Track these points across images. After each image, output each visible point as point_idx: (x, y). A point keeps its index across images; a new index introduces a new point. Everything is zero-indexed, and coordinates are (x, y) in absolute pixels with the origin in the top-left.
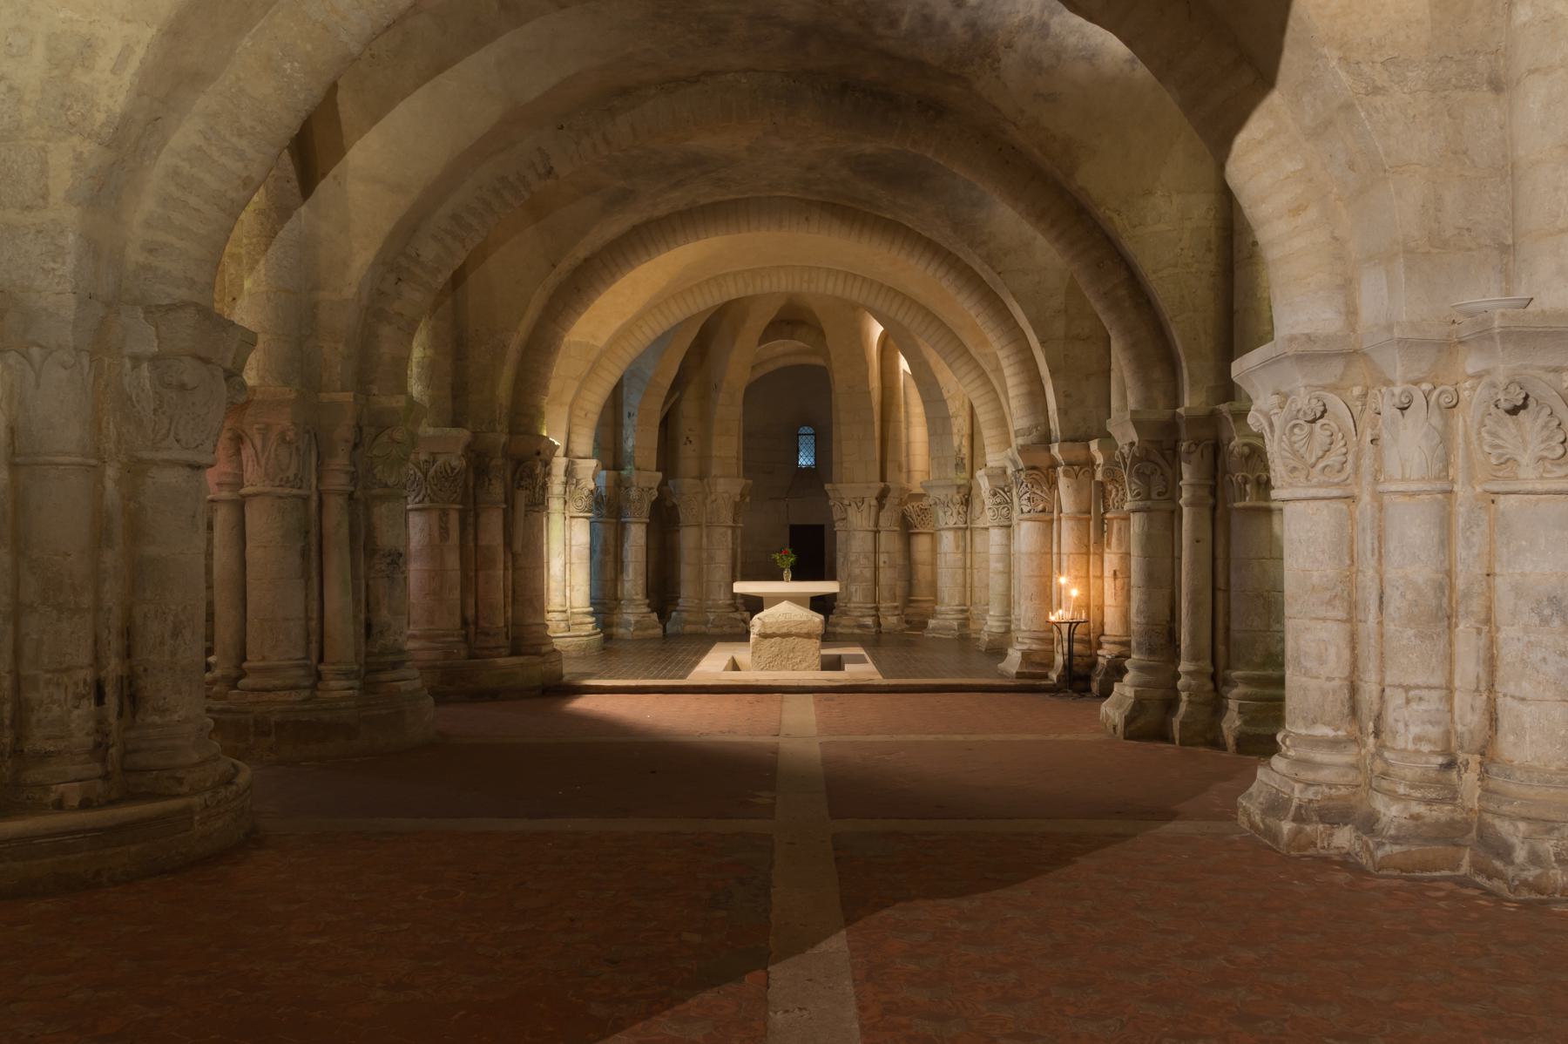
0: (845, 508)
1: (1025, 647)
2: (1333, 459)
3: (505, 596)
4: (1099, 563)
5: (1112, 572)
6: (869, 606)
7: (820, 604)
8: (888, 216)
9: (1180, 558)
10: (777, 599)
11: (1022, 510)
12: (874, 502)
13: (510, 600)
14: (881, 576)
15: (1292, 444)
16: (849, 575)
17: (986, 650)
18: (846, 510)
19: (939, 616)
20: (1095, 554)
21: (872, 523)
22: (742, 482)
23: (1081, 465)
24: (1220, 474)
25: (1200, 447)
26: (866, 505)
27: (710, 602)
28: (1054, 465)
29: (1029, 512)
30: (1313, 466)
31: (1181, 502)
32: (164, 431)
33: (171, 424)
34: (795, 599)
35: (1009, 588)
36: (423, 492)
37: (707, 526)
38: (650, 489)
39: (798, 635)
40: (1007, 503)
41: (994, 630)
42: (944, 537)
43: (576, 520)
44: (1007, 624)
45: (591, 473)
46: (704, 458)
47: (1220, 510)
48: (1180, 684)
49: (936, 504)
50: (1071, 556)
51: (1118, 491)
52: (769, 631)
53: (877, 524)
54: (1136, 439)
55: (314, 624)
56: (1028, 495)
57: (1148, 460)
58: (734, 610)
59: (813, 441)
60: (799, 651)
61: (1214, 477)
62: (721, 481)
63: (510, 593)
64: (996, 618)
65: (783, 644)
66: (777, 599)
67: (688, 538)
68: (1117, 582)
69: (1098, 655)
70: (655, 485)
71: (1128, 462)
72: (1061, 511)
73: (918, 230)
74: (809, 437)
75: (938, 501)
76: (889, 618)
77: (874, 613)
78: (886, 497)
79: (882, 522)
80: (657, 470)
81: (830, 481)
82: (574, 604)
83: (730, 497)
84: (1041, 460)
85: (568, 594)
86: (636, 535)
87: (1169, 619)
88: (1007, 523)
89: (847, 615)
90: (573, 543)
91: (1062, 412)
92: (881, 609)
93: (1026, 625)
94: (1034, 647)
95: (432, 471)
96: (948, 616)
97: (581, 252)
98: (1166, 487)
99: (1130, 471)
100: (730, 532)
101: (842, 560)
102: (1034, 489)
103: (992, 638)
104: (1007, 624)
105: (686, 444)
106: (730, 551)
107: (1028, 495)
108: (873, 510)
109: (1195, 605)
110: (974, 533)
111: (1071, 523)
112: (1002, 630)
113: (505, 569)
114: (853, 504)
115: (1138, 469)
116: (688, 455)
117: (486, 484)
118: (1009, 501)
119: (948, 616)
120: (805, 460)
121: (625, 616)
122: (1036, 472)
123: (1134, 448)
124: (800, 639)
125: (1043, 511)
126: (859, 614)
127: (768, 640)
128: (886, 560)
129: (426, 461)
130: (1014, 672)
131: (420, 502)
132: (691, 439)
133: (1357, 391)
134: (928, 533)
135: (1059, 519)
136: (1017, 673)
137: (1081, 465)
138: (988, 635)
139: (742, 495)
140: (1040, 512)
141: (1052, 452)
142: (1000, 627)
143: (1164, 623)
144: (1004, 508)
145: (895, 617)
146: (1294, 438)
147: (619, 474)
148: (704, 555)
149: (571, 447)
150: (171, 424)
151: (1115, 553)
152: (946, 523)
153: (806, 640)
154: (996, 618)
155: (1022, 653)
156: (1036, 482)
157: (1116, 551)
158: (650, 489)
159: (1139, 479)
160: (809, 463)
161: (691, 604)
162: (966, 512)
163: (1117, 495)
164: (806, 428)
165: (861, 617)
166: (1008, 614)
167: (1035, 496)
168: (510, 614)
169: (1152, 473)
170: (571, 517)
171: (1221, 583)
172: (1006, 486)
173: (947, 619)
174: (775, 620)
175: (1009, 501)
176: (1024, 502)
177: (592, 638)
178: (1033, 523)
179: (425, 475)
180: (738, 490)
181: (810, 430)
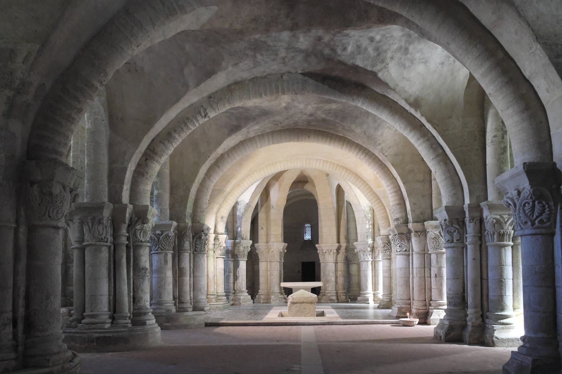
0: (324, 254)
1: (399, 306)
2: (544, 216)
3: (190, 288)
4: (429, 271)
5: (435, 275)
6: (334, 292)
7: (315, 290)
8: (341, 135)
9: (467, 267)
10: (298, 289)
11: (397, 251)
12: (335, 251)
13: (192, 289)
14: (338, 280)
15: (524, 211)
16: (326, 280)
18: (324, 254)
19: (362, 295)
20: (427, 268)
21: (335, 260)
22: (284, 244)
23: (421, 232)
24: (483, 231)
25: (474, 220)
26: (332, 252)
27: (271, 291)
28: (410, 232)
29: (400, 251)
30: (536, 219)
31: (467, 243)
32: (43, 213)
33: (46, 209)
34: (306, 289)
35: (391, 283)
36: (158, 246)
37: (270, 261)
38: (248, 247)
39: (307, 303)
40: (389, 250)
41: (385, 300)
42: (363, 264)
43: (218, 259)
45: (224, 240)
46: (268, 235)
47: (483, 246)
48: (468, 318)
49: (360, 251)
50: (417, 269)
51: (436, 242)
52: (295, 301)
53: (336, 260)
54: (447, 218)
55: (112, 297)
56: (399, 245)
57: (452, 226)
58: (280, 294)
59: (310, 229)
60: (307, 309)
61: (481, 233)
62: (276, 244)
63: (192, 286)
64: (386, 295)
66: (298, 289)
67: (262, 266)
68: (437, 278)
69: (429, 309)
70: (249, 246)
71: (444, 227)
72: (413, 251)
73: (353, 140)
74: (309, 228)
75: (360, 250)
76: (342, 297)
77: (336, 295)
78: (340, 249)
79: (338, 259)
80: (250, 240)
81: (318, 243)
82: (218, 292)
83: (279, 250)
84: (404, 230)
86: (243, 265)
87: (462, 292)
88: (389, 258)
89: (325, 296)
90: (218, 268)
91: (413, 211)
92: (339, 293)
93: (399, 297)
94: (403, 306)
95: (161, 237)
97: (220, 150)
98: (460, 237)
99: (445, 231)
100: (279, 264)
101: (323, 274)
102: (402, 242)
103: (384, 303)
104: (390, 298)
105: (261, 230)
106: (279, 271)
107: (399, 245)
108: (335, 255)
109: (474, 286)
110: (375, 262)
111: (417, 255)
112: (388, 300)
113: (190, 277)
114: (327, 252)
115: (448, 230)
116: (262, 233)
117: (183, 243)
118: (390, 249)
120: (308, 237)
121: (238, 297)
122: (403, 235)
123: (447, 222)
124: (307, 304)
125: (406, 251)
126: (330, 295)
127: (295, 305)
128: (341, 274)
129: (159, 234)
130: (395, 316)
131: (157, 250)
132: (263, 228)
133: (554, 186)
134: (357, 264)
135: (412, 254)
136: (396, 316)
137: (421, 232)
139: (283, 249)
140: (404, 251)
141: (409, 227)
142: (386, 299)
143: (461, 294)
144: (388, 252)
145: (344, 296)
146: (526, 208)
147: (235, 241)
148: (269, 273)
149: (216, 230)
150: (46, 209)
151: (436, 267)
152: (364, 259)
153: (310, 305)
154: (387, 296)
155: (398, 308)
156: (401, 239)
157: (436, 266)
158: (248, 247)
159: (448, 234)
160: (309, 238)
161: (264, 292)
162: (372, 254)
163: (436, 244)
164: (308, 224)
165: (331, 296)
166: (391, 294)
167: (403, 245)
168: (192, 295)
169: (454, 232)
170: (217, 258)
171: (484, 276)
172: (388, 243)
175: (390, 249)
176: (398, 248)
177: (225, 305)
178: (401, 256)
179: (159, 240)
180: (282, 247)
181: (309, 225)
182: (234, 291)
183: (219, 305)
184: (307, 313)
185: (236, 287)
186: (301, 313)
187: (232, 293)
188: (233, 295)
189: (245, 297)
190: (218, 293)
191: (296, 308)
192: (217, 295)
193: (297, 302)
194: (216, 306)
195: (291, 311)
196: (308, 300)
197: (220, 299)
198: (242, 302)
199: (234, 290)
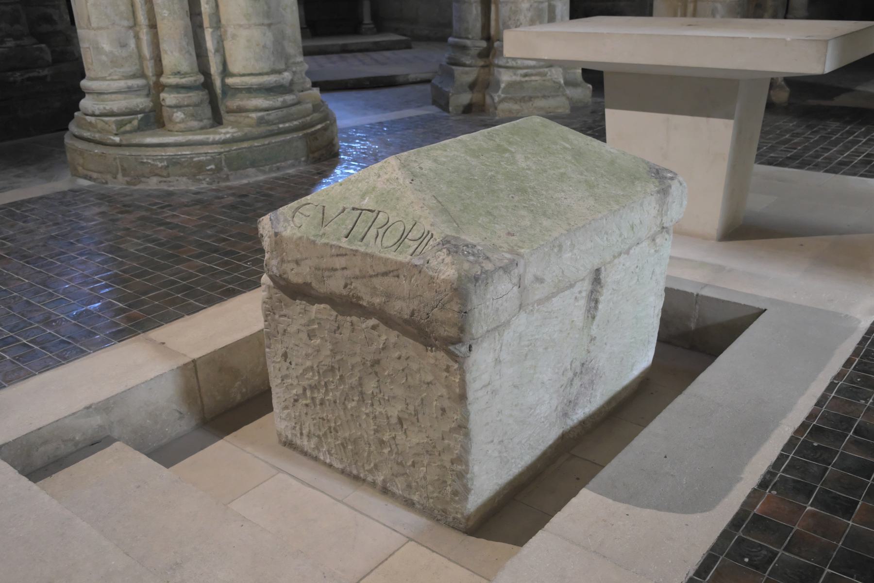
65: (346, 332)
82: (234, 68)
85: (210, 44)
127: (299, 305)
177: (245, 145)
182: (484, 44)
183: (187, 152)
185: (497, 20)
187: (474, 52)
188: (481, 63)
189: (526, 75)
190: (233, 75)
191: (311, 335)
192: (226, 88)
194: (171, 151)
197: (240, 110)
198: (502, 101)
199: (488, 38)
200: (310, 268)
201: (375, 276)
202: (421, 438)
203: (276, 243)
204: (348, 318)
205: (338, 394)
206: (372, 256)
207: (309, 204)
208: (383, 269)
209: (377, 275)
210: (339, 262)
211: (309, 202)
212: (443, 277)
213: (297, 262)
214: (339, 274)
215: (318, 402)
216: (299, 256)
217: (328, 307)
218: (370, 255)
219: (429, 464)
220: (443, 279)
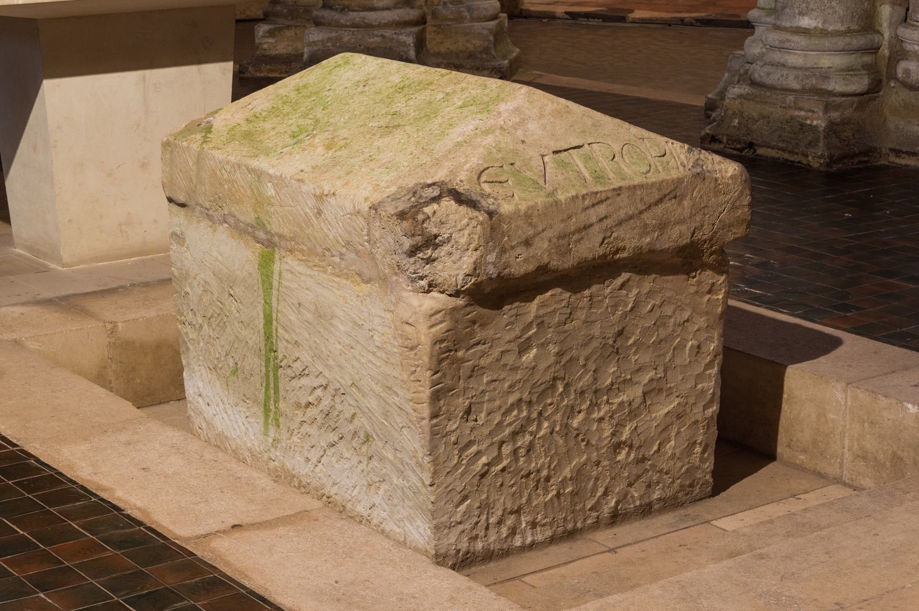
17: (832, 161)
41: (835, 85)
44: (867, 59)
64: (841, 42)
65: (581, 315)
96: (372, 16)
104: (867, 59)
112: (860, 84)
119: (372, 16)
124: (648, 283)
138: (827, 108)
153: (670, 284)
154: (841, 42)
173: (369, 26)
174: (540, 200)
184: (637, 392)
186: (572, 411)
191: (523, 349)
193: (543, 269)
195: (462, 403)
196: (663, 226)
200: (550, 241)
201: (645, 210)
202: (672, 404)
203: (493, 229)
204: (587, 292)
205: (558, 417)
206: (641, 186)
207: (488, 168)
208: (657, 196)
209: (649, 207)
210: (593, 215)
211: (486, 166)
212: (729, 174)
213: (527, 243)
214: (596, 228)
215: (522, 451)
216: (531, 232)
217: (559, 290)
218: (639, 186)
219: (678, 433)
220: (731, 176)
